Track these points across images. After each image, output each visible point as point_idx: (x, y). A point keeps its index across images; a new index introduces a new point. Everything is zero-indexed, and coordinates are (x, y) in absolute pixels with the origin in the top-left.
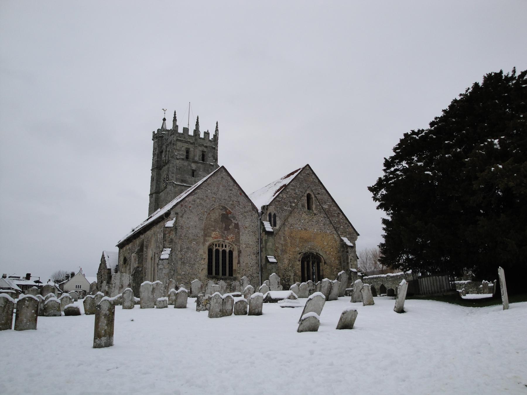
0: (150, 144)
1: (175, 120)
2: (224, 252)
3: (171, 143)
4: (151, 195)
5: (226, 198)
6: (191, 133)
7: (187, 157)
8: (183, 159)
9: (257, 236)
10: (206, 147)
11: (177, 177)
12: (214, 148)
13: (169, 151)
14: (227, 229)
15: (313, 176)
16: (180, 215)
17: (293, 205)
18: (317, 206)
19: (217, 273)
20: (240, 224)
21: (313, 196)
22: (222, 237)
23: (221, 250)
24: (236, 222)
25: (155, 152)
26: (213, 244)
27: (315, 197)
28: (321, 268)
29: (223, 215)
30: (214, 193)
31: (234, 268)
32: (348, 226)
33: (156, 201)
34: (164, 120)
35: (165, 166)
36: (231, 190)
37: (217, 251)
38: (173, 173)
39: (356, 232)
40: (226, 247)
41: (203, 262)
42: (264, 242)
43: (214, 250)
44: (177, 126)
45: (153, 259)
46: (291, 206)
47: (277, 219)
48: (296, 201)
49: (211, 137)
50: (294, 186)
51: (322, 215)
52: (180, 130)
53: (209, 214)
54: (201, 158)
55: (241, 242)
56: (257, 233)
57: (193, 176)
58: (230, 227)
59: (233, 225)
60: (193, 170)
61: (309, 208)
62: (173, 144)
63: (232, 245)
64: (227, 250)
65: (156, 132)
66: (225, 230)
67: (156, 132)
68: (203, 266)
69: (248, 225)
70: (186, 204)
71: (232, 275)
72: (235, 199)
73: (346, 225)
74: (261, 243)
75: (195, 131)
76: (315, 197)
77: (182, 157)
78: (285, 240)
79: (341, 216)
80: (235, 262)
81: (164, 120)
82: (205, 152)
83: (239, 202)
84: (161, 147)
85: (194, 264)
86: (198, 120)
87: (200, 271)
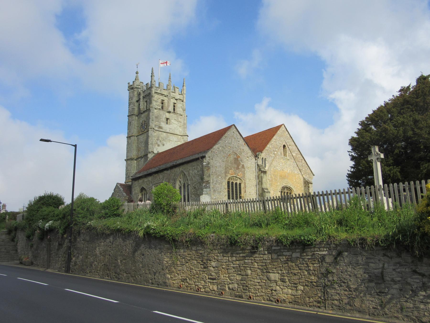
2: (236, 183)
7: (162, 108)
10: (176, 100)
15: (287, 132)
17: (276, 153)
21: (287, 147)
22: (235, 173)
23: (234, 183)
24: (243, 164)
25: (131, 101)
29: (235, 158)
34: (137, 73)
35: (142, 113)
37: (232, 183)
38: (153, 120)
45: (182, 188)
58: (240, 167)
61: (285, 155)
64: (238, 182)
70: (214, 150)
72: (242, 148)
77: (159, 107)
78: (271, 177)
81: (137, 73)
85: (220, 192)
86: (170, 76)
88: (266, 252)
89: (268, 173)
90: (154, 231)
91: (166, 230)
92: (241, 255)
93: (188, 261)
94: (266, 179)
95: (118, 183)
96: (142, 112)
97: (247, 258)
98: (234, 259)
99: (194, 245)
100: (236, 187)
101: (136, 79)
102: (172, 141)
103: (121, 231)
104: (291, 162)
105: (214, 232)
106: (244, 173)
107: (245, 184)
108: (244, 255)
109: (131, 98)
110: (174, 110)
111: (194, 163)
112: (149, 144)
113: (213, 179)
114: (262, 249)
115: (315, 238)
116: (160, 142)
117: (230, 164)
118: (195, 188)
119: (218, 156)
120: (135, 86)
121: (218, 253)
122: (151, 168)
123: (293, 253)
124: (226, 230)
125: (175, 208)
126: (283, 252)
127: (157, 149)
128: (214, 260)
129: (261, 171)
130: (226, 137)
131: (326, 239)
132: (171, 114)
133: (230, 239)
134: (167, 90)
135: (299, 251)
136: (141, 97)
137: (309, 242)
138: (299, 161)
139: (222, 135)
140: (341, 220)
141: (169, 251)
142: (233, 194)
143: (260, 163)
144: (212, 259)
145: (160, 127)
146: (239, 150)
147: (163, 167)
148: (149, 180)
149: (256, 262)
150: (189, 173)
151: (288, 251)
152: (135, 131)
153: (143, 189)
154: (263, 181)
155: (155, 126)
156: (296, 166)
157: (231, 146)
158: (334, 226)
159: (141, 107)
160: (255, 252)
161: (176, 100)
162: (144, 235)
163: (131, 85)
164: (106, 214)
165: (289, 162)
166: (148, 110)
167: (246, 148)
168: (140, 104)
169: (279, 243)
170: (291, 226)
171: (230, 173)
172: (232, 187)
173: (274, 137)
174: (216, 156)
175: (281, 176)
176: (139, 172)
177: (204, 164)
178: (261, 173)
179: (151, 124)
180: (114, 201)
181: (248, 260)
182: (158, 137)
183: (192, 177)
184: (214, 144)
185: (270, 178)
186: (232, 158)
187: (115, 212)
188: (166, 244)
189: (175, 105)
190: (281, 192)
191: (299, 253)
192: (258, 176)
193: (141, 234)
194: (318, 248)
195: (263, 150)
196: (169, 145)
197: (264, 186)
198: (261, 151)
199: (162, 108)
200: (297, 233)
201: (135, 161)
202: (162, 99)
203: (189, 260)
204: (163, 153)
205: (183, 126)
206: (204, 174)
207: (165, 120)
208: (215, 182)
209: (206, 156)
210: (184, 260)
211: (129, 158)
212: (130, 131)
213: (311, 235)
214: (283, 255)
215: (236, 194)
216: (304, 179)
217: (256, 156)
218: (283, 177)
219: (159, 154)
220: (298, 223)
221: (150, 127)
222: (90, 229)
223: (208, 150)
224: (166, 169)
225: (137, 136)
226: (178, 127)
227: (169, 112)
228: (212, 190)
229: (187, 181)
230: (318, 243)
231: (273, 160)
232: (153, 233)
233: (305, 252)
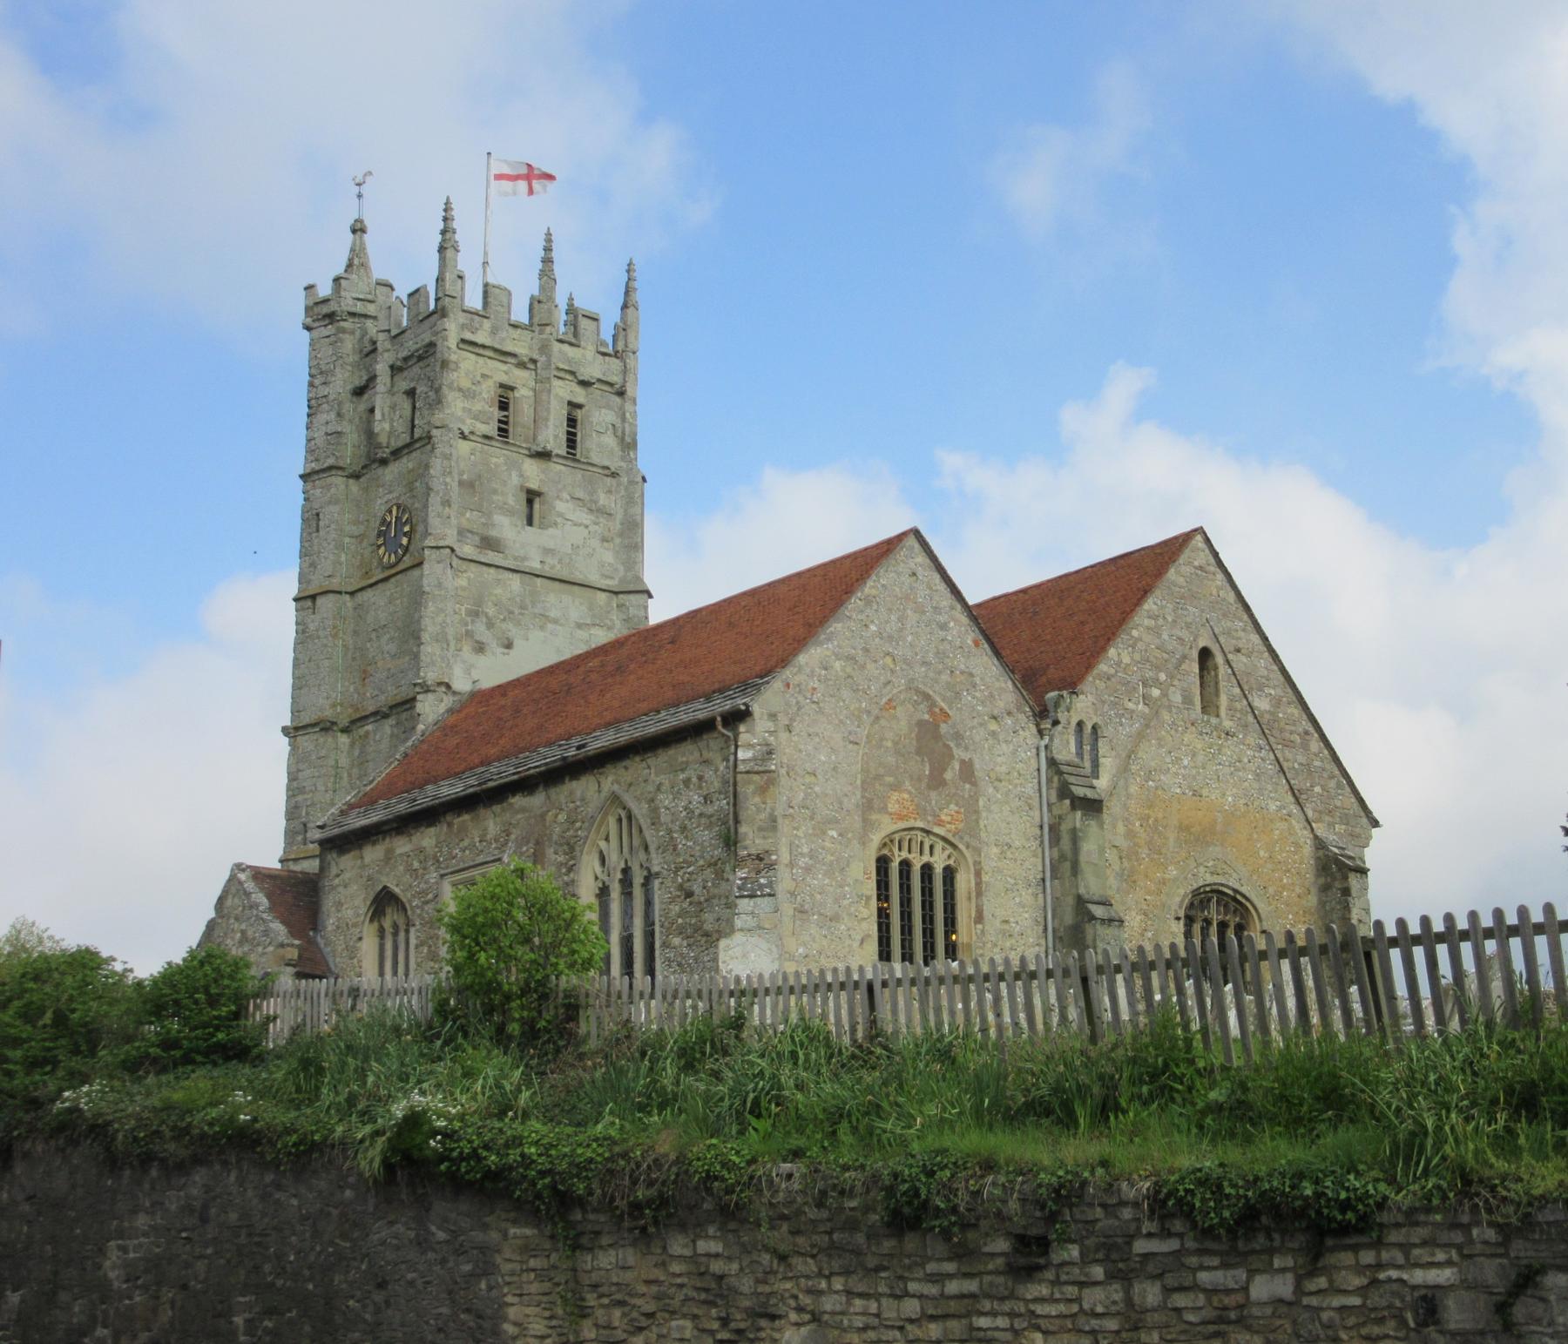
0: (293, 347)
1: (447, 246)
2: (927, 870)
5: (931, 657)
7: (503, 432)
8: (486, 437)
9: (1037, 813)
10: (585, 384)
11: (465, 524)
15: (1220, 576)
16: (783, 720)
17: (1156, 692)
18: (1232, 700)
20: (977, 766)
21: (1219, 659)
22: (921, 812)
24: (966, 756)
25: (324, 391)
27: (1228, 662)
29: (921, 723)
30: (890, 637)
32: (1339, 786)
34: (358, 229)
35: (384, 462)
37: (905, 865)
38: (447, 503)
40: (931, 854)
41: (865, 912)
43: (895, 865)
47: (1103, 747)
48: (1162, 677)
50: (1155, 618)
51: (1250, 740)
52: (474, 300)
53: (877, 718)
54: (564, 437)
55: (983, 835)
56: (1036, 803)
57: (530, 522)
58: (948, 775)
59: (957, 766)
61: (1209, 705)
64: (939, 862)
66: (929, 787)
67: (325, 290)
68: (864, 925)
69: (1004, 769)
72: (960, 663)
73: (1332, 784)
75: (535, 302)
76: (1228, 662)
78: (1130, 834)
81: (358, 229)
82: (580, 406)
83: (971, 675)
85: (835, 918)
86: (548, 249)
87: (856, 944)
88: (1098, 1272)
89: (1113, 808)
90: (450, 1144)
91: (517, 1141)
92: (953, 1287)
93: (644, 1322)
94: (1101, 844)
95: (239, 867)
96: (385, 453)
97: (987, 1305)
98: (911, 1307)
99: (682, 1227)
100: (927, 892)
101: (350, 265)
102: (555, 621)
103: (257, 1142)
104: (1247, 750)
105: (797, 1154)
106: (972, 810)
107: (978, 874)
108: (972, 1286)
109: (319, 375)
110: (571, 442)
111: (686, 753)
112: (425, 637)
113: (790, 845)
114: (1074, 1252)
115: (1382, 1187)
116: (490, 625)
117: (891, 760)
118: (689, 894)
119: (821, 711)
120: (347, 304)
121: (820, 1274)
122: (435, 780)
123: (1252, 1273)
124: (868, 1139)
125: (572, 1009)
126: (1194, 1270)
127: (468, 671)
128: (793, 1316)
129: (1073, 800)
130: (868, 601)
131: (1445, 1198)
132: (556, 468)
133: (890, 1191)
134: (529, 328)
135: (1290, 1262)
136: (382, 368)
137: (1350, 1215)
138: (1288, 744)
139: (849, 591)
140: (1533, 1084)
141: (532, 1263)
142: (907, 929)
143: (1065, 748)
144: (782, 1309)
145: (489, 543)
146: (945, 677)
147: (504, 772)
148: (422, 850)
149: (1038, 1328)
150: (654, 812)
151: (1225, 1266)
152: (340, 566)
153: (384, 901)
154: (1083, 858)
155: (462, 532)
156: (1271, 768)
157: (898, 652)
158: (1492, 1120)
159: (381, 426)
160: (1039, 1268)
161: (585, 384)
162: (388, 1166)
163: (325, 301)
164: (168, 1044)
165: (1230, 750)
166: (418, 442)
167: (985, 667)
168: (372, 410)
169: (1172, 1216)
170: (1239, 1116)
171: (893, 807)
172: (905, 888)
173: (1149, 605)
175: (1183, 828)
176: (368, 801)
177: (741, 755)
178: (1073, 807)
179: (434, 522)
180: (217, 970)
181: (993, 1314)
182: (479, 602)
183: (670, 832)
184: (800, 643)
185: (1121, 842)
186: (902, 722)
187: (220, 1036)
188: (515, 1222)
189: (579, 414)
190: (1189, 920)
191: (1290, 1277)
192: (1054, 830)
193: (371, 1160)
194: (1400, 1246)
195: (1081, 678)
196: (535, 652)
197: (1090, 885)
198: (1072, 685)
199: (503, 432)
200: (1272, 1156)
201: (344, 739)
202: (504, 379)
203: (650, 1315)
204: (502, 689)
205: (621, 535)
206: (743, 815)
207: (517, 502)
208: (802, 862)
209: (756, 709)
210: (617, 1313)
211: (306, 721)
212: (313, 565)
213: (1358, 1174)
214: (1195, 1287)
215: (929, 933)
216: (1319, 844)
217: (1043, 714)
218: (1198, 836)
219: (481, 698)
220: (1283, 1097)
221: (429, 542)
222: (71, 1128)
223: (767, 673)
224: (525, 785)
225: (352, 594)
226: (595, 543)
227: (544, 455)
228: (788, 909)
229: (642, 855)
230: (1400, 1218)
231: (1140, 736)
232: (442, 1158)
233: (1327, 1271)
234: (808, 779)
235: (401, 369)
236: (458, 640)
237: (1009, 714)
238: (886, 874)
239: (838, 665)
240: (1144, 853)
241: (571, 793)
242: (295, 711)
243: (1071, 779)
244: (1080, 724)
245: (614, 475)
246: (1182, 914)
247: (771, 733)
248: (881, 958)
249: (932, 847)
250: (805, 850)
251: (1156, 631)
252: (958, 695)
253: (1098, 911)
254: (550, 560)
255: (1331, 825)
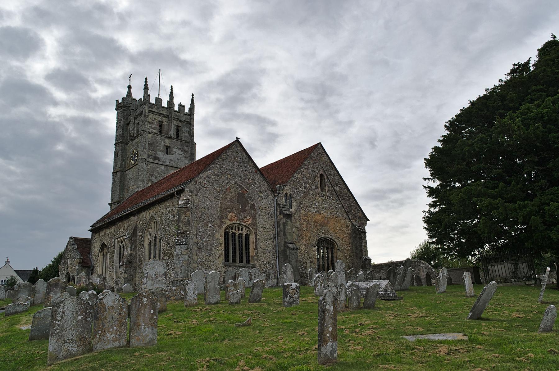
1: (146, 88)
2: (241, 235)
3: (141, 114)
4: (114, 173)
6: (165, 104)
7: (160, 132)
10: (180, 121)
11: (150, 153)
12: (190, 124)
13: (138, 123)
14: (243, 210)
17: (308, 185)
18: (329, 188)
19: (234, 261)
21: (326, 177)
22: (238, 219)
25: (120, 124)
26: (230, 227)
27: (328, 178)
28: (335, 255)
29: (239, 194)
31: (251, 254)
32: (358, 210)
33: (121, 179)
34: (130, 87)
35: (132, 140)
36: (246, 167)
37: (234, 234)
38: (144, 148)
39: (366, 217)
42: (282, 226)
44: (149, 96)
45: (153, 244)
46: (305, 187)
48: (310, 181)
49: (187, 110)
50: (308, 166)
52: (153, 101)
55: (258, 225)
58: (247, 208)
60: (166, 146)
62: (145, 116)
63: (249, 228)
65: (120, 101)
67: (120, 101)
68: (220, 252)
71: (249, 263)
73: (356, 210)
74: (278, 225)
76: (328, 178)
77: (154, 131)
78: (301, 224)
79: (351, 200)
80: (252, 247)
81: (130, 87)
84: (127, 118)
85: (211, 250)
86: (172, 90)
87: (217, 258)
95: (71, 238)
106: (254, 218)
107: (256, 236)
110: (178, 135)
111: (169, 203)
116: (156, 178)
117: (229, 204)
118: (169, 244)
130: (223, 159)
138: (344, 199)
148: (111, 232)
150: (161, 220)
153: (103, 246)
155: (149, 156)
157: (232, 174)
161: (180, 121)
163: (121, 103)
174: (203, 189)
185: (299, 226)
186: (233, 193)
189: (180, 129)
202: (160, 120)
205: (190, 156)
209: (186, 190)
216: (353, 225)
218: (320, 225)
227: (170, 138)
234: (202, 210)
235: (136, 118)
236: (147, 181)
237: (266, 191)
238: (228, 237)
239: (213, 177)
240: (305, 229)
241: (143, 215)
242: (112, 199)
243: (283, 209)
244: (286, 194)
245: (188, 143)
246: (316, 245)
247: (190, 196)
248: (225, 261)
249: (242, 229)
250: (201, 230)
251: (308, 169)
252: (250, 186)
253: (290, 246)
254: (171, 162)
255: (356, 221)
